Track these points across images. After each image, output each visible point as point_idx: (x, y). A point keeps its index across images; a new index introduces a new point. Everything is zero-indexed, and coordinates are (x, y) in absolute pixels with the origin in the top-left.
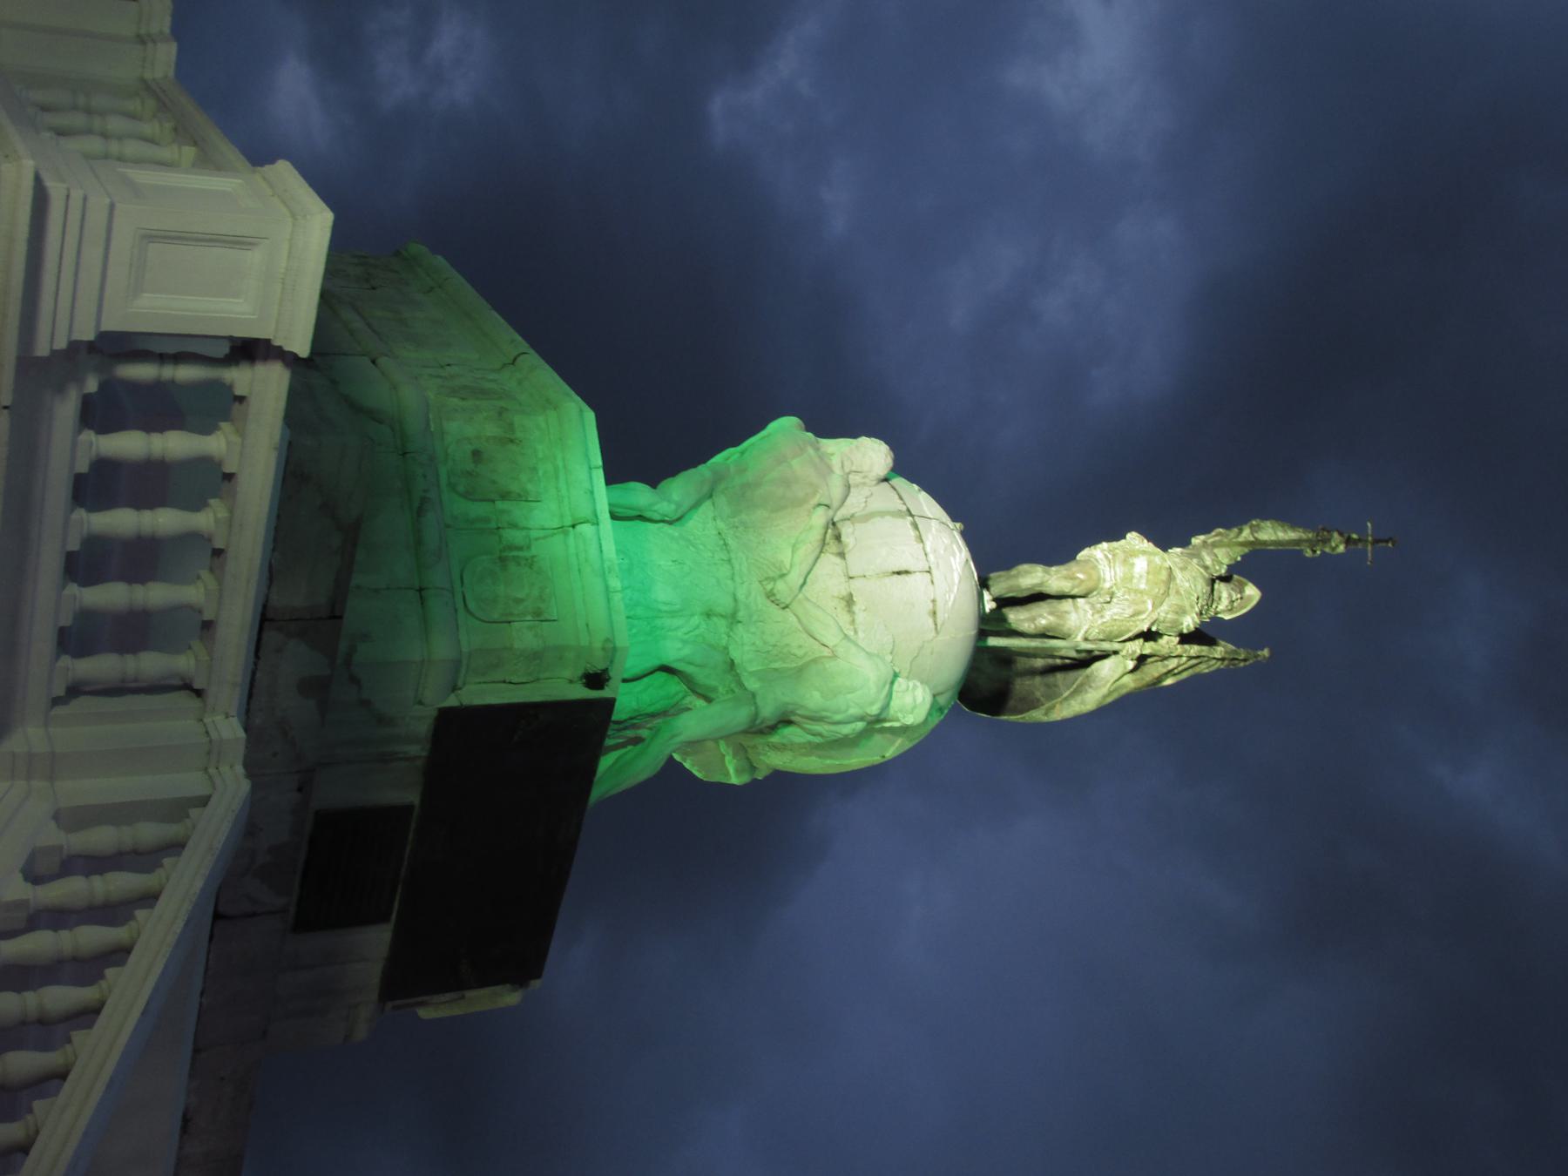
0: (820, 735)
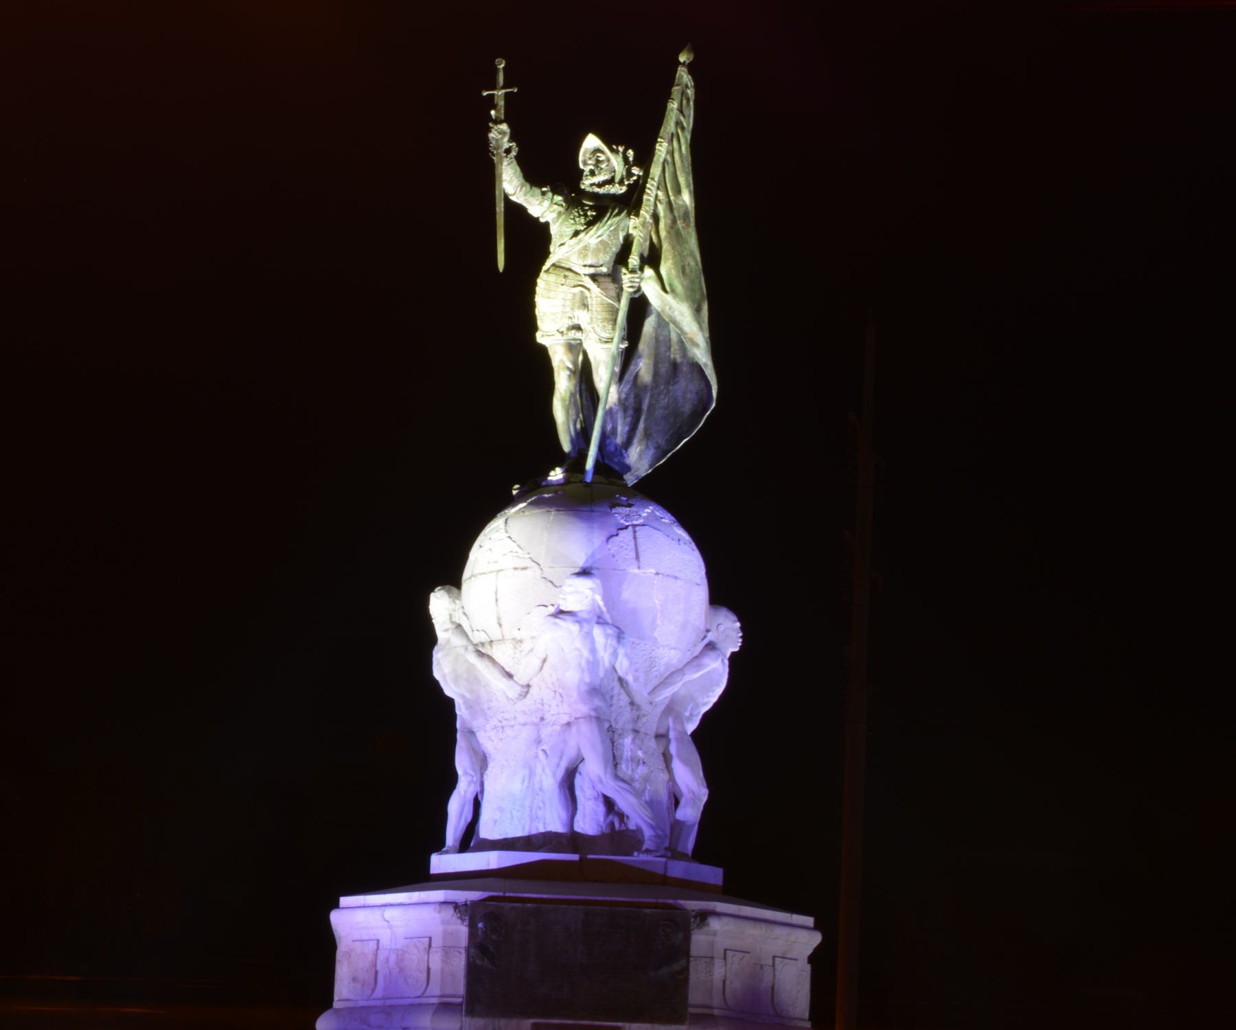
0: (615, 654)
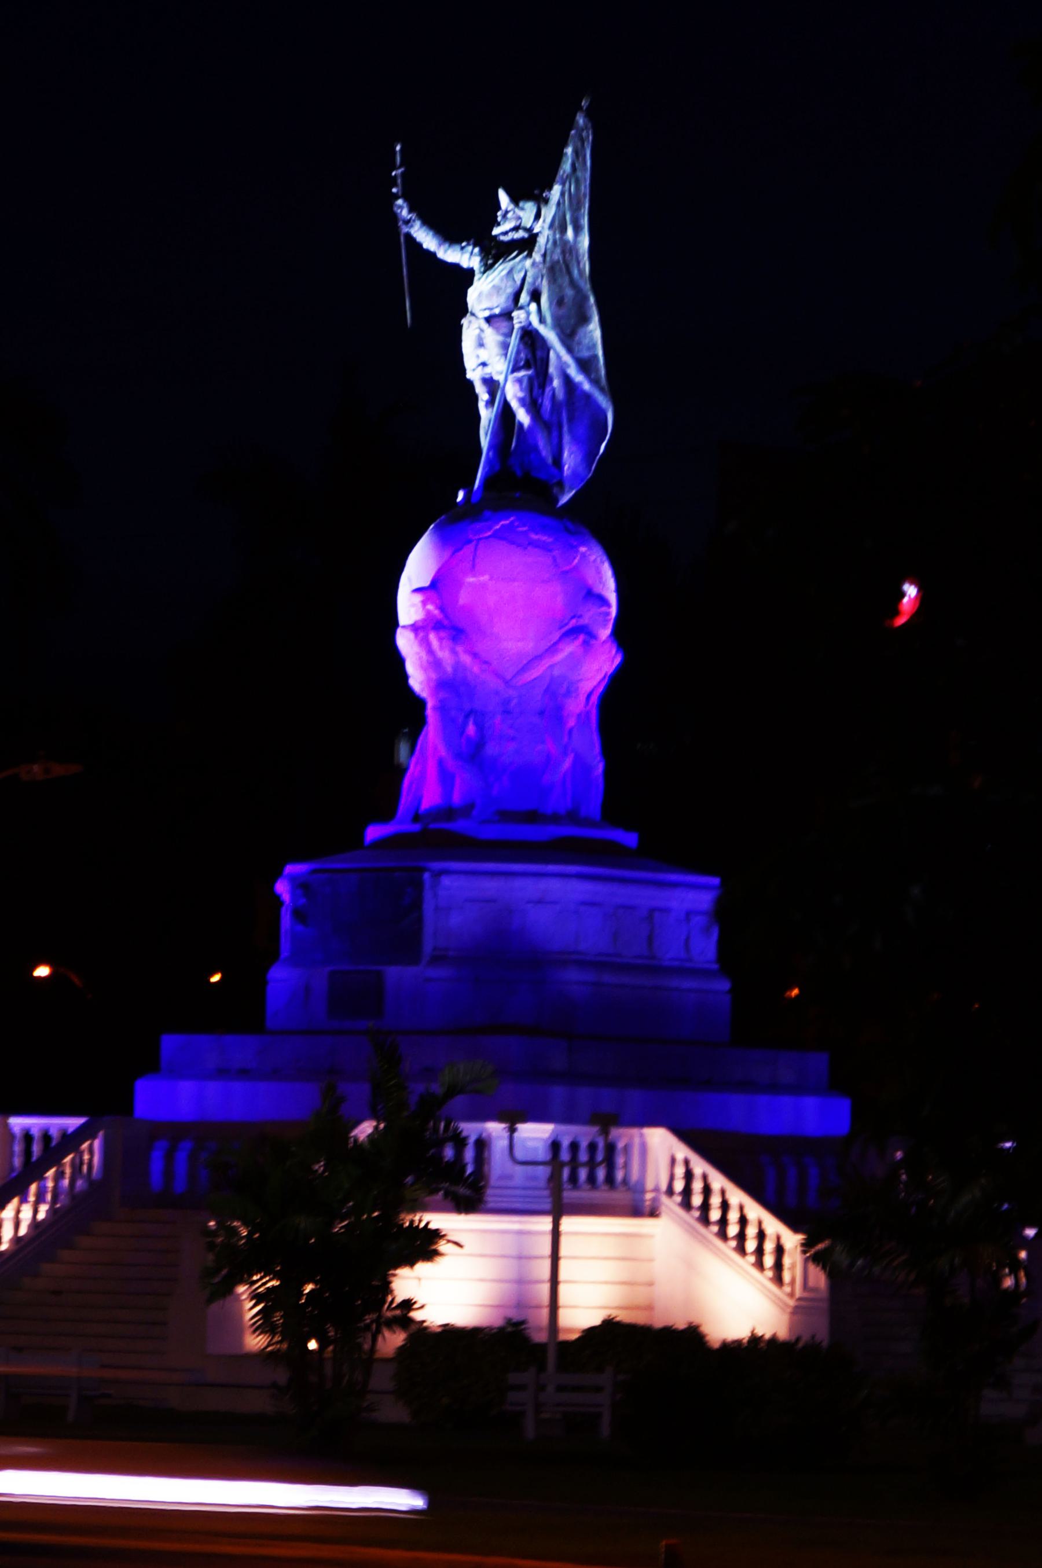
0: (454, 652)
